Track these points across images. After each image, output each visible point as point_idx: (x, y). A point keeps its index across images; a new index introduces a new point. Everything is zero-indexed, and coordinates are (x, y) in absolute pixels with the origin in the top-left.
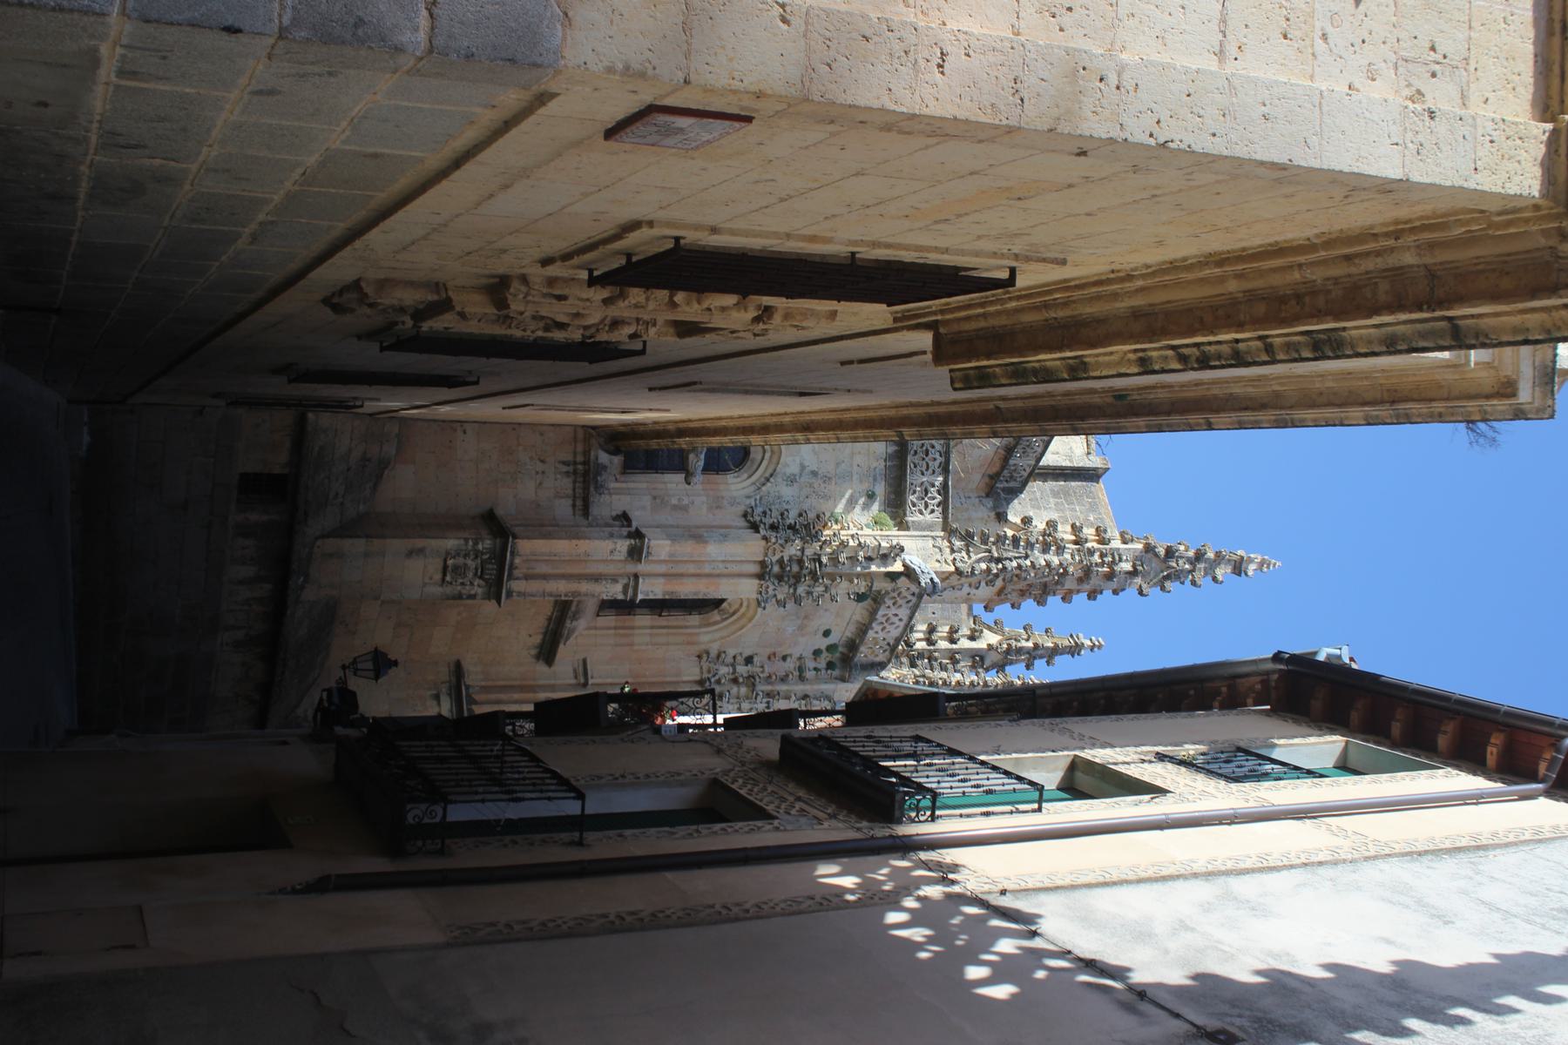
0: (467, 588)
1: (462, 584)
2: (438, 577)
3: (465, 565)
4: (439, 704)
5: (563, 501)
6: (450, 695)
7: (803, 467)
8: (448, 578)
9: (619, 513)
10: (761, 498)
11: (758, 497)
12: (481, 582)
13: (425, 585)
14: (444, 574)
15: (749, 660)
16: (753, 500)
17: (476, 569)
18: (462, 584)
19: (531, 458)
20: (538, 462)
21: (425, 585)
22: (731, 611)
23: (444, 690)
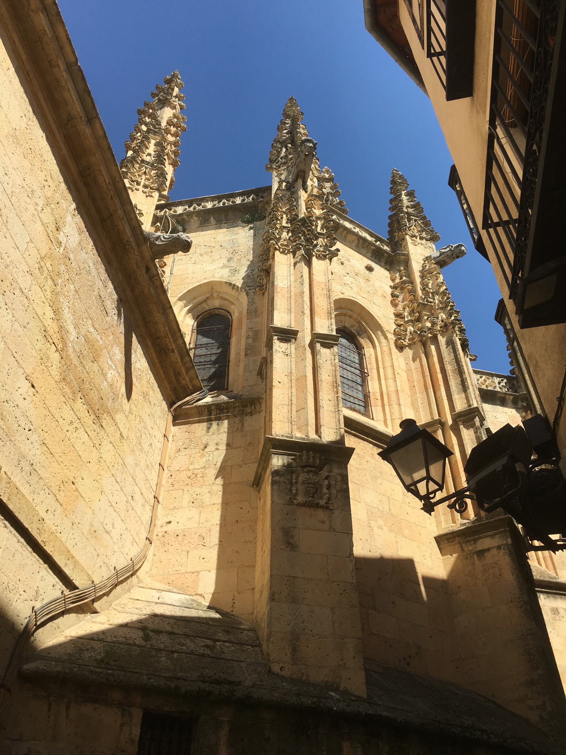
0: (333, 483)
1: (329, 487)
2: (321, 514)
3: (303, 483)
4: (488, 550)
5: (246, 424)
6: (475, 541)
7: (224, 266)
8: (322, 502)
9: (259, 377)
10: (248, 287)
11: (248, 288)
12: (326, 468)
13: (332, 529)
14: (318, 506)
15: (398, 316)
16: (249, 291)
17: (308, 472)
18: (329, 487)
19: (202, 456)
20: (207, 450)
21: (332, 529)
22: (358, 325)
23: (470, 548)
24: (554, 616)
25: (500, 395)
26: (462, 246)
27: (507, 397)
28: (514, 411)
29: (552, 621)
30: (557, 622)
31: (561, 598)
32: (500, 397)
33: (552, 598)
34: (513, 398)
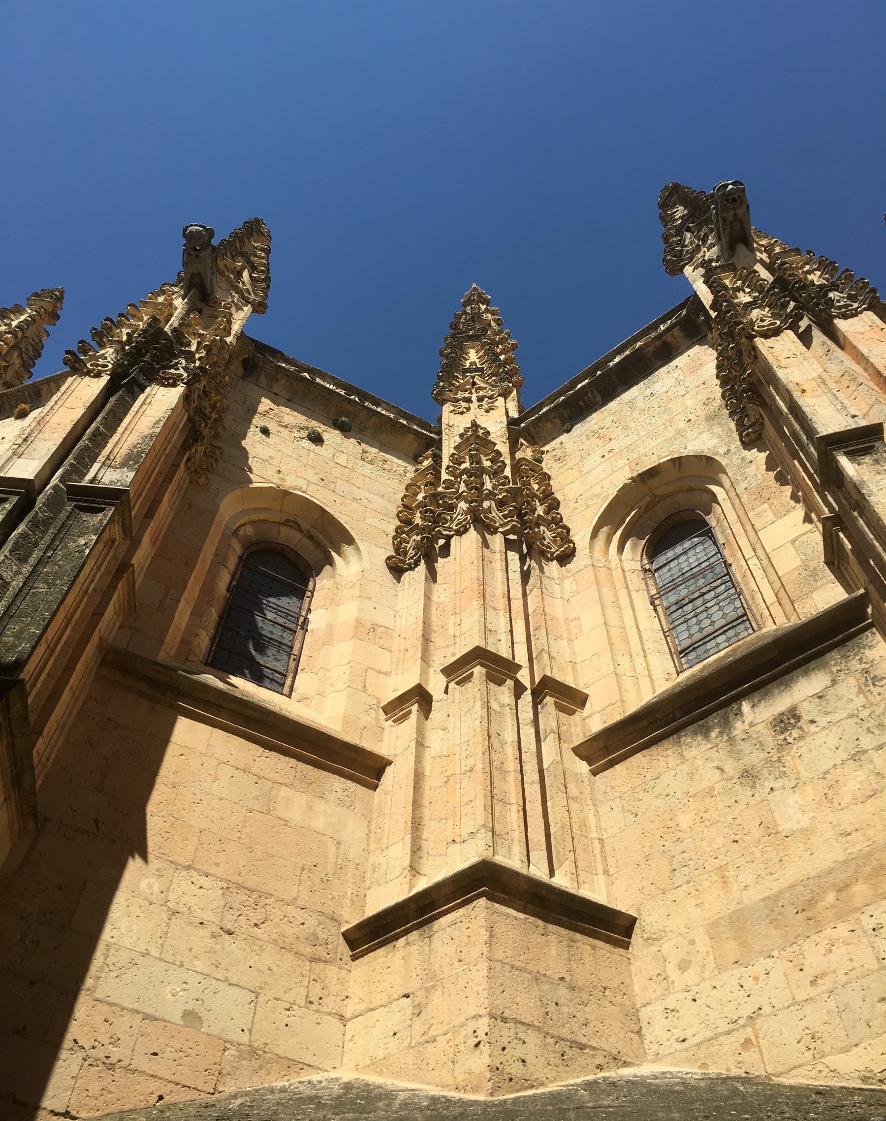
24: (783, 737)
25: (651, 349)
26: (187, 228)
27: (668, 338)
28: (696, 349)
29: (775, 758)
30: (795, 748)
31: (806, 673)
32: (655, 353)
33: (776, 691)
34: (683, 329)
